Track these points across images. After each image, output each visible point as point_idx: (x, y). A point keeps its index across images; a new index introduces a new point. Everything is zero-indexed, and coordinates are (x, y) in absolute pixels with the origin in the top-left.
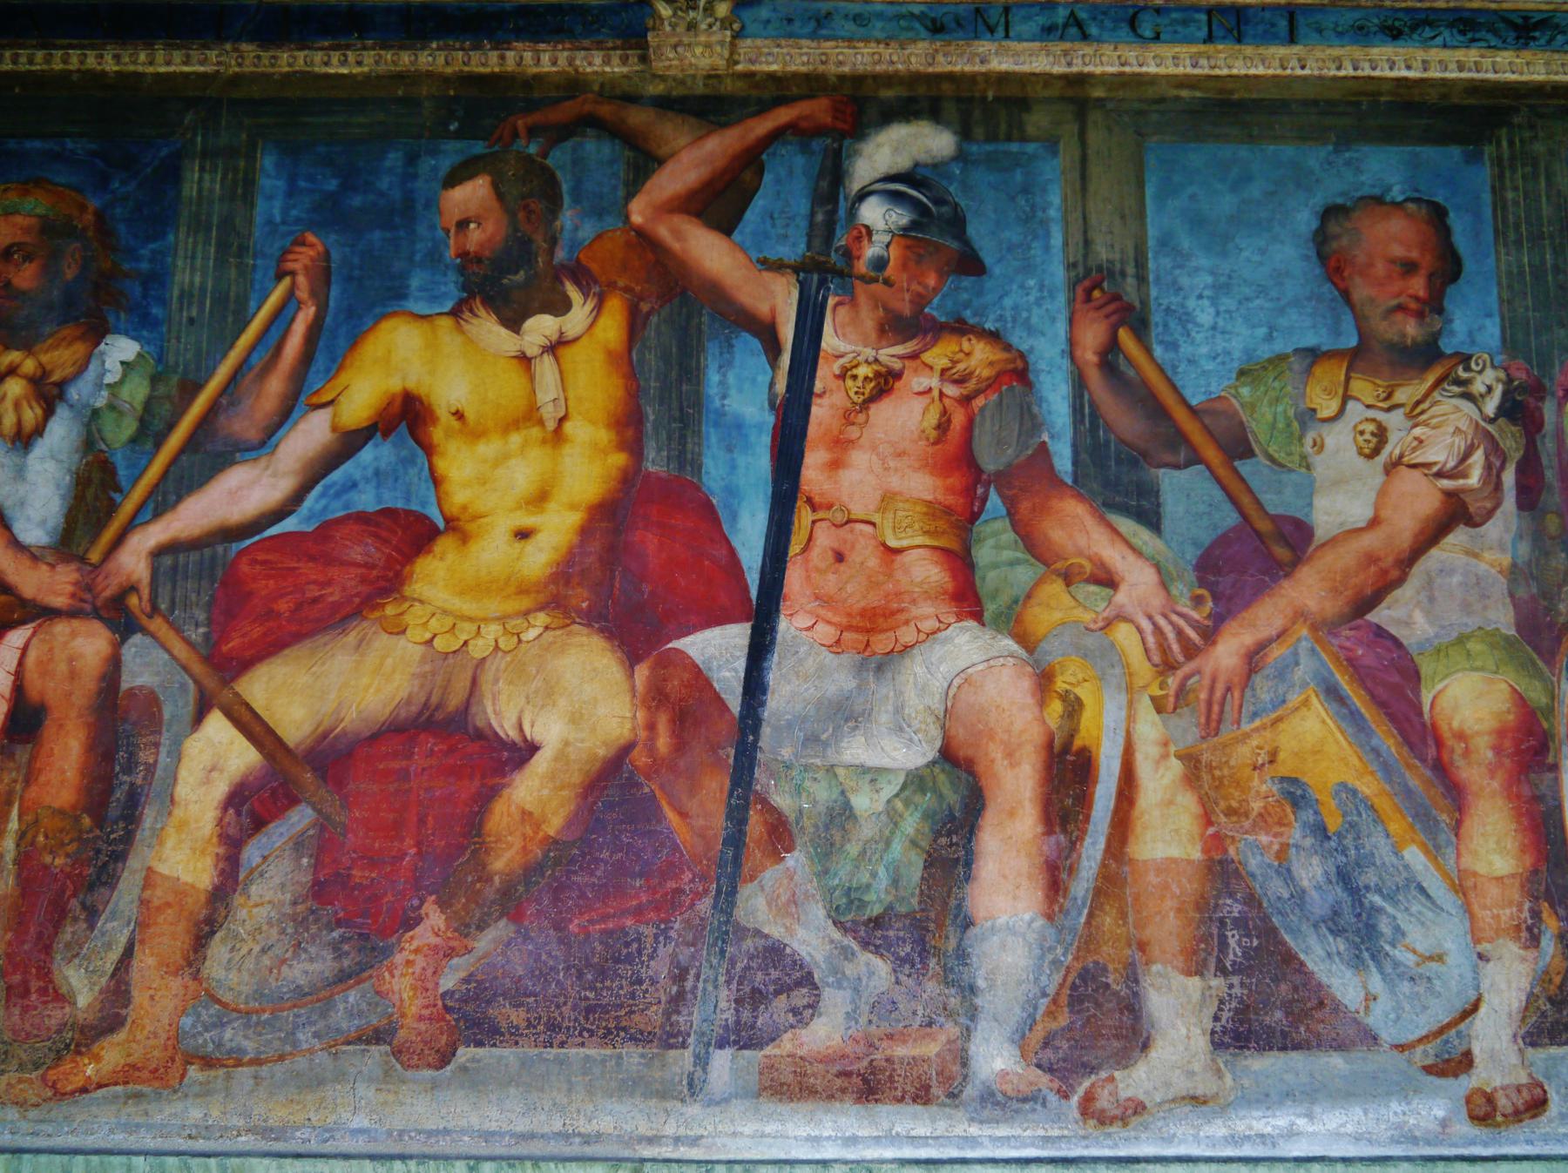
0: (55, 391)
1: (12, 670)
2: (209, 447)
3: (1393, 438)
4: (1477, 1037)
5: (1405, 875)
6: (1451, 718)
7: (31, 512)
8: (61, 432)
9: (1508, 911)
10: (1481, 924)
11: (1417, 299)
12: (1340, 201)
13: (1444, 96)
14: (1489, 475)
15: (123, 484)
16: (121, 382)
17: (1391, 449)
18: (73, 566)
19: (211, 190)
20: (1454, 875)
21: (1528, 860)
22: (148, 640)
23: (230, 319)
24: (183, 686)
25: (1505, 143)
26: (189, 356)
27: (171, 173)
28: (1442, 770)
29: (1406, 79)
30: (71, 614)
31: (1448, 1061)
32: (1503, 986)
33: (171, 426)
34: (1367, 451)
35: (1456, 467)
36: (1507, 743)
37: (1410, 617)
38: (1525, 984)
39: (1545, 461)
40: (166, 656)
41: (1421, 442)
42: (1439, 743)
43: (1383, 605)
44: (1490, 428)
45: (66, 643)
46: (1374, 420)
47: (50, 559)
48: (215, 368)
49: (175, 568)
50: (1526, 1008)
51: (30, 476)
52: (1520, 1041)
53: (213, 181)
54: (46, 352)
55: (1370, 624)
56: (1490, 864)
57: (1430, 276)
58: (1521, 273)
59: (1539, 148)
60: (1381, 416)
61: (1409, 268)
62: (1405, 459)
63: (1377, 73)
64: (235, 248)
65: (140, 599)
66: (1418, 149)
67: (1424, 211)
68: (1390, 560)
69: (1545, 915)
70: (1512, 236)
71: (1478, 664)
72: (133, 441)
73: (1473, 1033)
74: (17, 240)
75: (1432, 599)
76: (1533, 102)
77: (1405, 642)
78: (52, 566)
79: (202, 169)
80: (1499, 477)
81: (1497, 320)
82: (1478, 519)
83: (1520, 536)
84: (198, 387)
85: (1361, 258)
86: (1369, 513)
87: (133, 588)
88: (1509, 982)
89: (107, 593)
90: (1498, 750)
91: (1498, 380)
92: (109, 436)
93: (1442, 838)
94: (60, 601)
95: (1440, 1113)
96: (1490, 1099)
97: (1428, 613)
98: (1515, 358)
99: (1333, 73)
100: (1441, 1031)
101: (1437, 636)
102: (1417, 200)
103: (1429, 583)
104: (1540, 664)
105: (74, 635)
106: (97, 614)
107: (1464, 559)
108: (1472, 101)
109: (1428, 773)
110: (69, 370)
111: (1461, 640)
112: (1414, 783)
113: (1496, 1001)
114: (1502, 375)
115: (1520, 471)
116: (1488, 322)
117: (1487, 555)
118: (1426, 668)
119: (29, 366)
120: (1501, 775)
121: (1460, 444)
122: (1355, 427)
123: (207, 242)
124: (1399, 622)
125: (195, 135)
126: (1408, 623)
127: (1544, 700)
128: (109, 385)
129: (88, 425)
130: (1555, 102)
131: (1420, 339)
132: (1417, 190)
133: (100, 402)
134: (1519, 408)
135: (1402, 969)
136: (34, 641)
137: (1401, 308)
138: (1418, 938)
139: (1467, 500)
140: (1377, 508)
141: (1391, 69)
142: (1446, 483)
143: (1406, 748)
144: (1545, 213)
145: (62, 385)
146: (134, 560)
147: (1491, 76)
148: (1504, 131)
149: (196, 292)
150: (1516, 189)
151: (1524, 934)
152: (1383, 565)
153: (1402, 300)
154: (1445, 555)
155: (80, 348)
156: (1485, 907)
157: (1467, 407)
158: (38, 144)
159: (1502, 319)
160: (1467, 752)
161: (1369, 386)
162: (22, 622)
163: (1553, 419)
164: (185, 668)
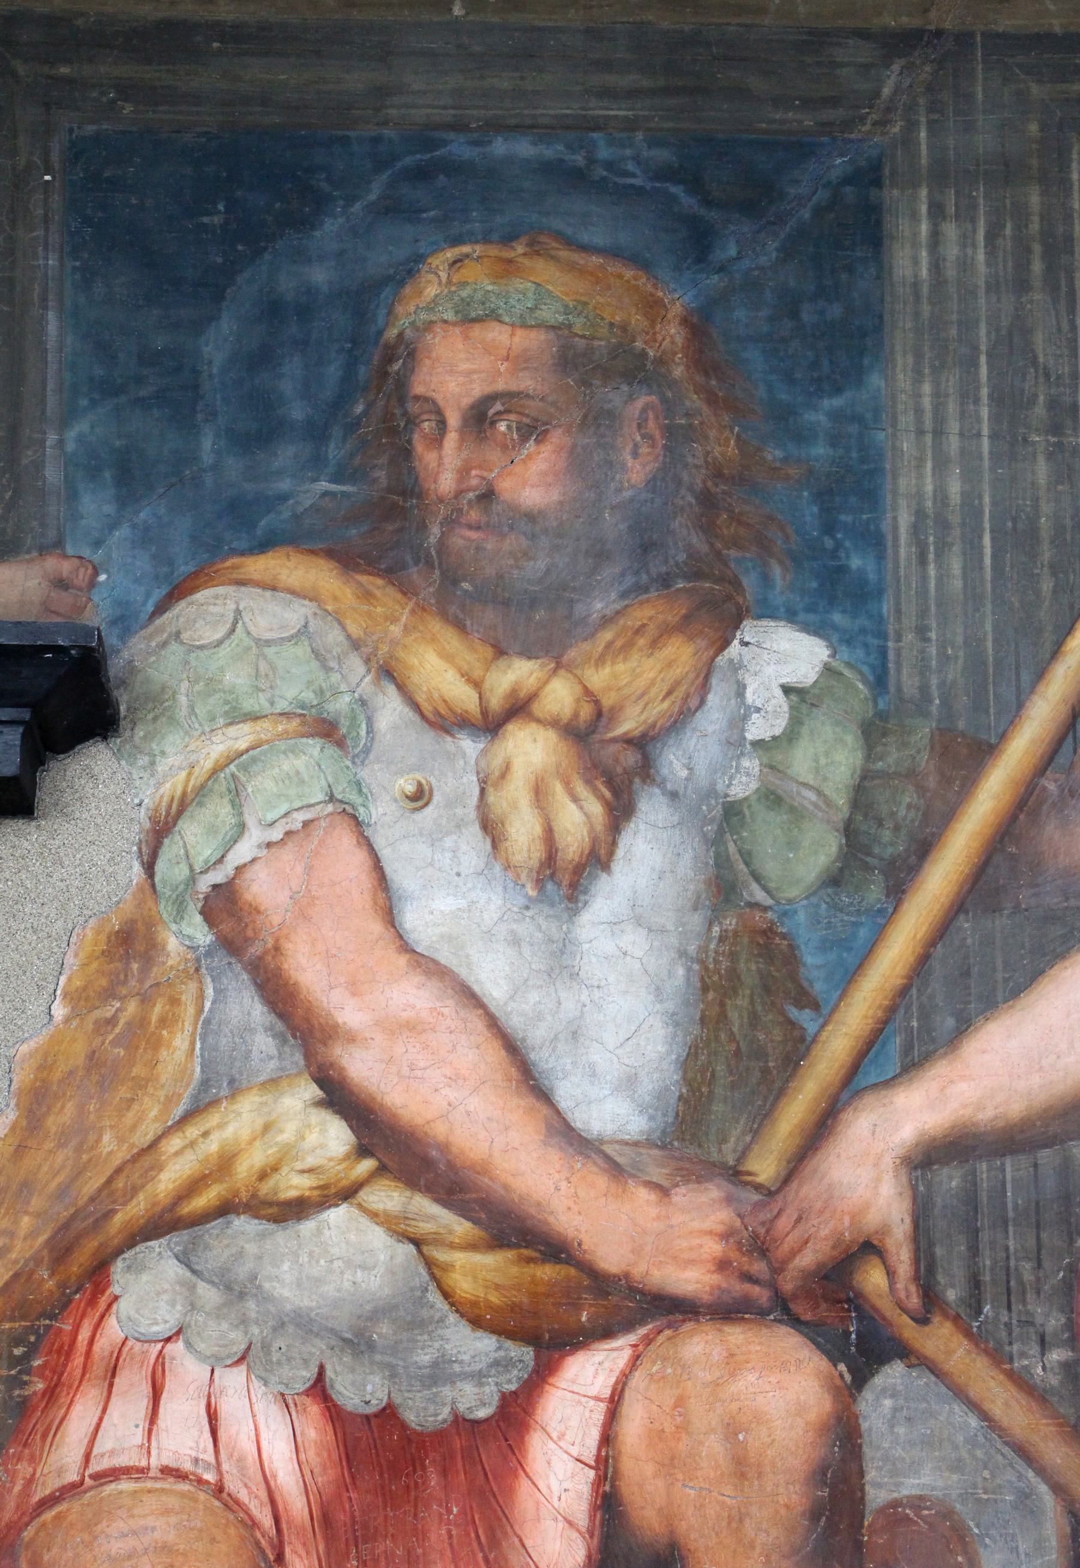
0: (631, 758)
1: (590, 1456)
2: (1025, 897)
7: (597, 1056)
8: (653, 859)
15: (819, 988)
16: (790, 737)
18: (714, 1191)
19: (965, 265)
22: (922, 1380)
23: (1047, 585)
24: (1025, 1496)
26: (954, 672)
27: (856, 227)
30: (727, 1311)
33: (924, 848)
40: (973, 1422)
45: (716, 1384)
47: (657, 1174)
48: (1020, 706)
49: (970, 1197)
51: (591, 967)
53: (967, 240)
54: (600, 661)
64: (1040, 410)
65: (891, 1274)
72: (834, 880)
74: (500, 386)
78: (663, 1191)
79: (937, 211)
84: (982, 752)
87: (870, 1248)
89: (807, 1260)
92: (770, 868)
94: (691, 1280)
105: (733, 1364)
106: (782, 1310)
110: (659, 709)
119: (560, 696)
123: (968, 395)
125: (911, 126)
128: (758, 744)
129: (716, 842)
133: (744, 782)
136: (638, 1380)
145: (644, 744)
146: (866, 1173)
149: (955, 519)
155: (681, 654)
158: (525, 148)
162: (604, 1332)
164: (1024, 1452)
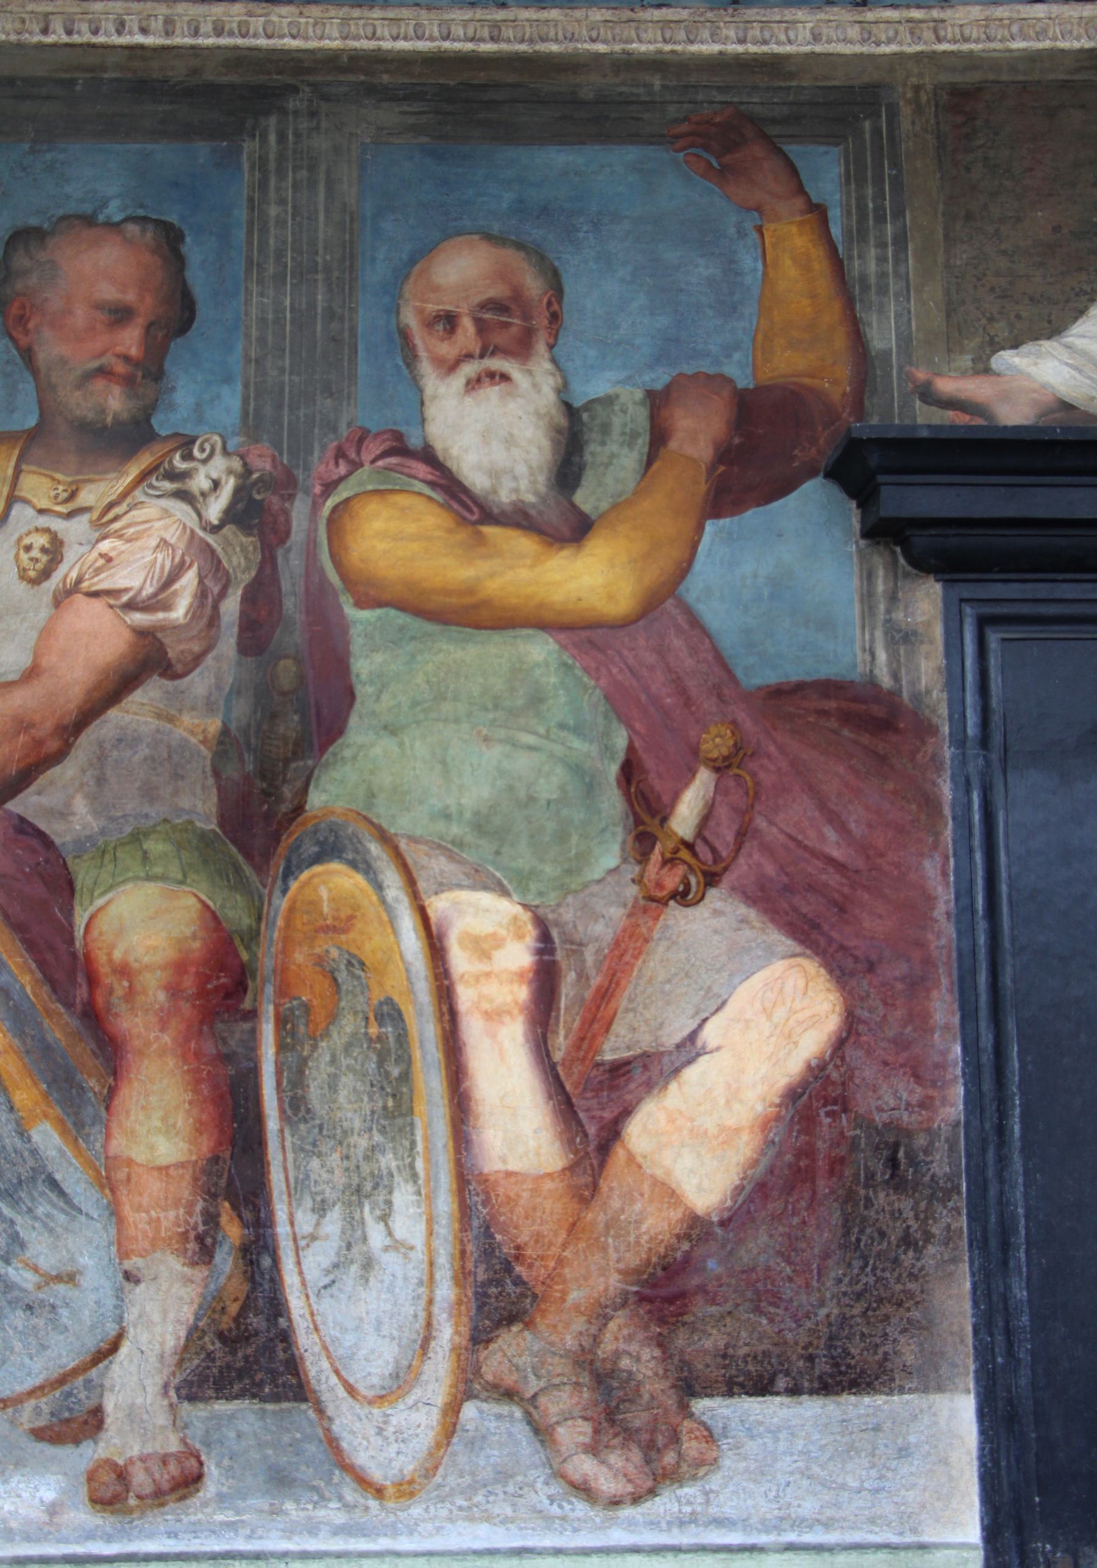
3: (71, 555)
4: (112, 1390)
5: (31, 1163)
6: (112, 947)
9: (172, 1214)
10: (132, 1232)
11: (127, 359)
12: (34, 221)
13: (195, 72)
14: (202, 605)
17: (67, 571)
20: (100, 1164)
21: (206, 1145)
25: (272, 138)
28: (94, 1021)
29: (141, 47)
31: (68, 1421)
32: (156, 1317)
34: (32, 574)
35: (155, 595)
36: (189, 983)
37: (68, 804)
38: (188, 1313)
39: (285, 585)
41: (109, 560)
42: (93, 981)
43: (33, 788)
44: (210, 539)
46: (47, 530)
50: (186, 1348)
52: (172, 1393)
55: (10, 814)
56: (152, 1148)
57: (149, 327)
58: (279, 321)
59: (321, 143)
60: (57, 525)
61: (120, 315)
62: (85, 585)
63: (101, 39)
66: (149, 147)
67: (149, 235)
68: (49, 725)
69: (224, 1220)
70: (271, 268)
71: (158, 870)
73: (107, 1383)
75: (101, 781)
76: (319, 78)
77: (58, 841)
80: (216, 607)
81: (239, 387)
82: (179, 668)
83: (236, 691)
85: (55, 303)
86: (25, 660)
88: (165, 1313)
90: (174, 991)
91: (230, 472)
93: (88, 1112)
95: (49, 1495)
96: (122, 1475)
97: (92, 799)
98: (257, 441)
99: (37, 38)
100: (62, 1380)
101: (103, 832)
102: (143, 220)
103: (101, 758)
104: (248, 870)
107: (154, 723)
108: (234, 78)
109: (75, 1023)
111: (137, 837)
112: (56, 1035)
113: (144, 1338)
114: (237, 464)
115: (250, 598)
116: (226, 391)
117: (187, 719)
118: (83, 874)
120: (176, 1025)
121: (165, 561)
122: (20, 539)
124: (51, 813)
126: (64, 814)
127: (246, 921)
130: (351, 78)
131: (125, 416)
132: (142, 206)
134: (255, 512)
135: (16, 1293)
137: (103, 372)
138: (43, 1252)
139: (167, 641)
140: (37, 655)
141: (119, 32)
142: (138, 618)
143: (46, 988)
144: (321, 236)
147: (262, 42)
148: (273, 121)
150: (282, 202)
151: (192, 1246)
152: (39, 733)
153: (108, 360)
154: (128, 718)
156: (139, 1208)
157: (181, 510)
159: (246, 386)
160: (131, 994)
161: (46, 483)
163: (305, 525)
